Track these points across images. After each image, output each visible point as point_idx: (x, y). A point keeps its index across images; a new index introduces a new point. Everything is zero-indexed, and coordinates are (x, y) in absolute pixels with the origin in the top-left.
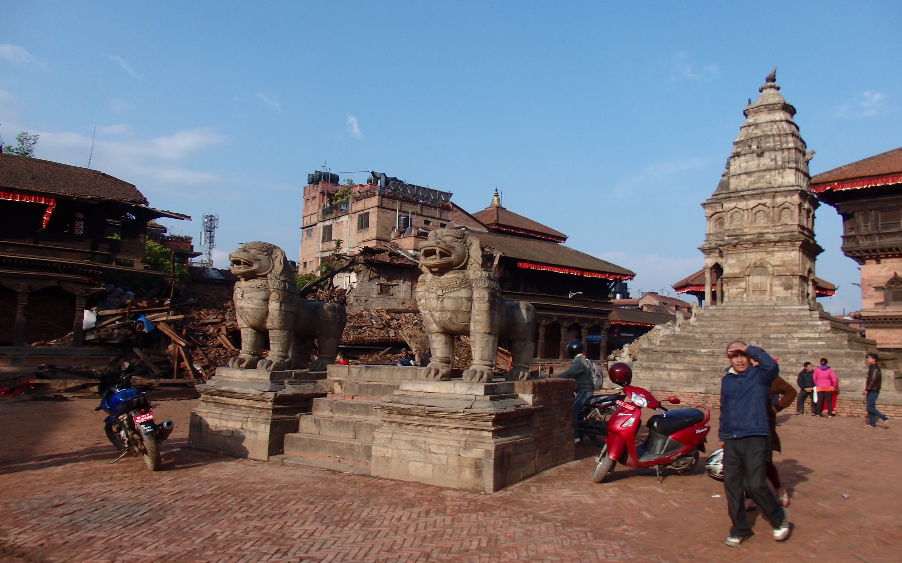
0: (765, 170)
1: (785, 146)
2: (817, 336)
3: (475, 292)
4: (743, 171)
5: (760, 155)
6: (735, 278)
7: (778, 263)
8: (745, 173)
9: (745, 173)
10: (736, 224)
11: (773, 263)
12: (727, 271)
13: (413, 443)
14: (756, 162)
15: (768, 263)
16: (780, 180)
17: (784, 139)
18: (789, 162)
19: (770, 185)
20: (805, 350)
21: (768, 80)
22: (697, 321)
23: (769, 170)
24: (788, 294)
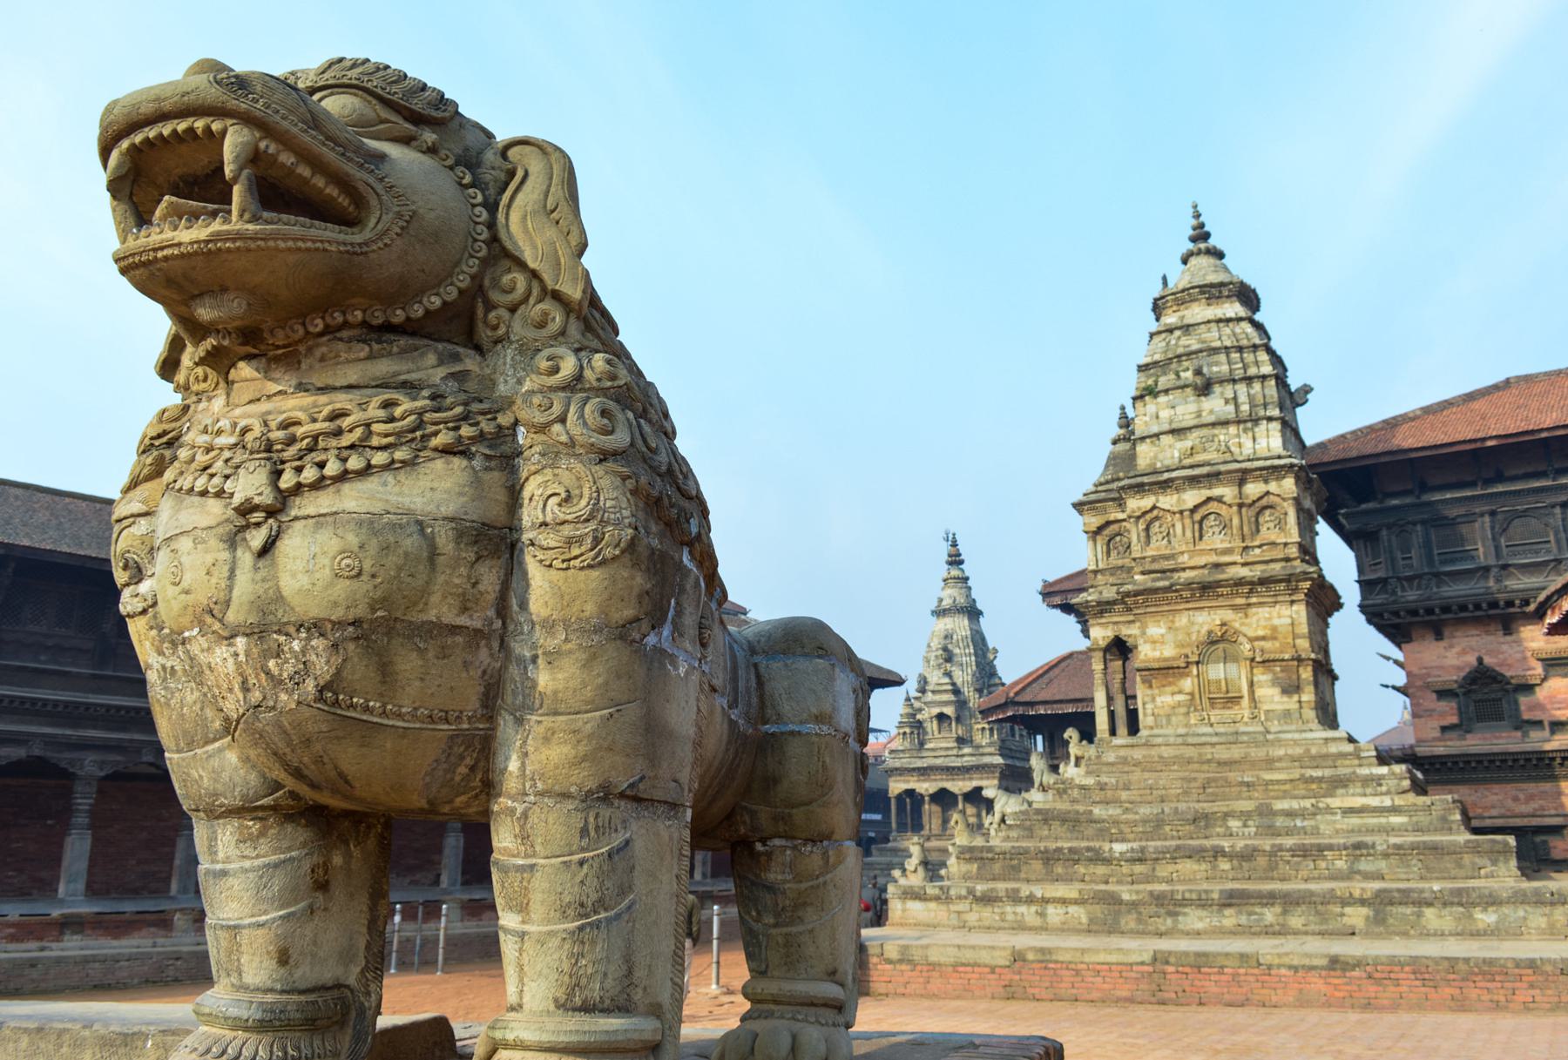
0: (1214, 425)
1: (1252, 371)
2: (1387, 802)
3: (532, 488)
4: (1166, 427)
5: (1205, 389)
6: (1165, 672)
7: (1261, 633)
8: (1172, 432)
9: (1172, 432)
10: (1157, 546)
11: (1251, 634)
12: (1146, 653)
17: (1249, 357)
18: (1265, 406)
19: (1228, 457)
20: (1368, 839)
21: (1193, 239)
22: (1088, 773)
24: (1291, 703)
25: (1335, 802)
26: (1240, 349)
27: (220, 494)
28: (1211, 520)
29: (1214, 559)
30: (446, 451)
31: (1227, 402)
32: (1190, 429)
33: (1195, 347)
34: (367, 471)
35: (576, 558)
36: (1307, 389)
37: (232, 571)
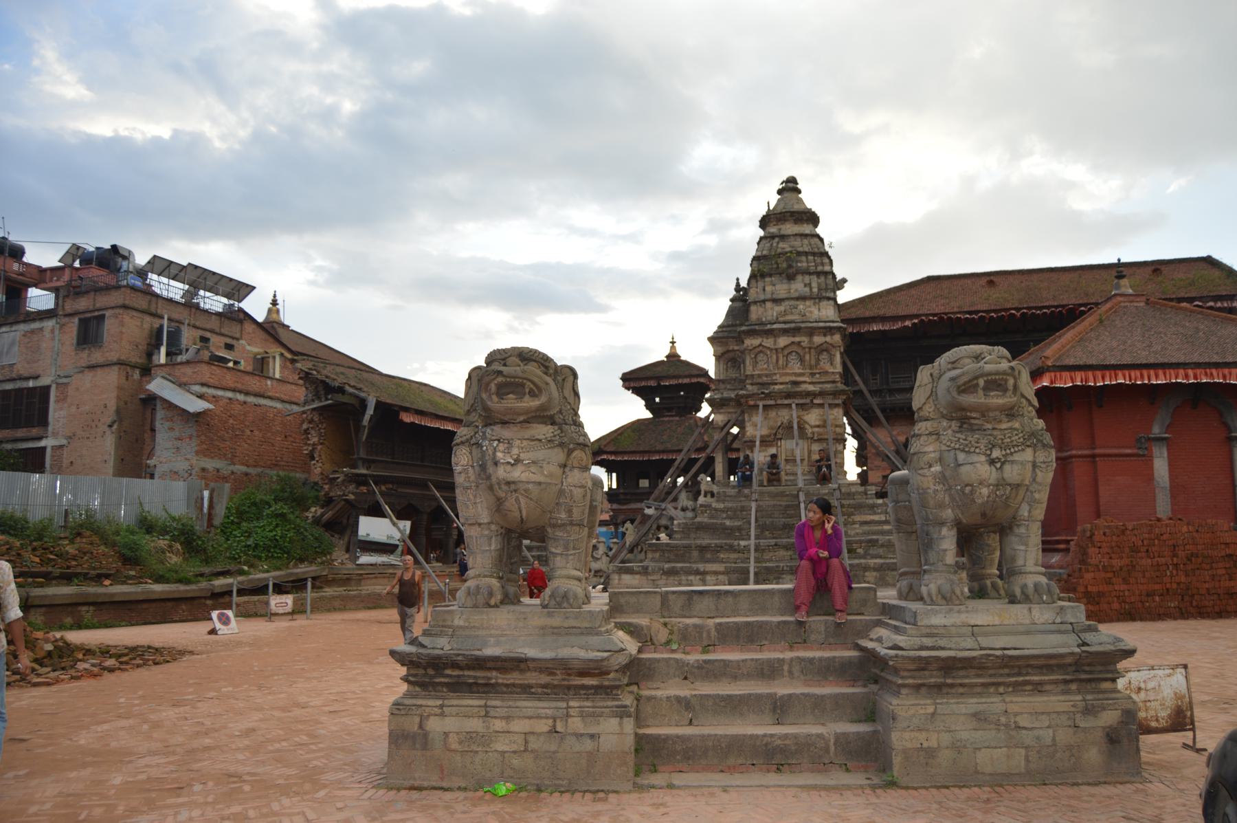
0: (797, 299)
1: (820, 268)
4: (769, 296)
11: (813, 423)
13: (979, 718)
14: (785, 286)
16: (816, 312)
17: (818, 260)
23: (803, 298)
25: (858, 518)
26: (814, 254)
28: (793, 356)
29: (794, 378)
33: (788, 249)
36: (844, 281)
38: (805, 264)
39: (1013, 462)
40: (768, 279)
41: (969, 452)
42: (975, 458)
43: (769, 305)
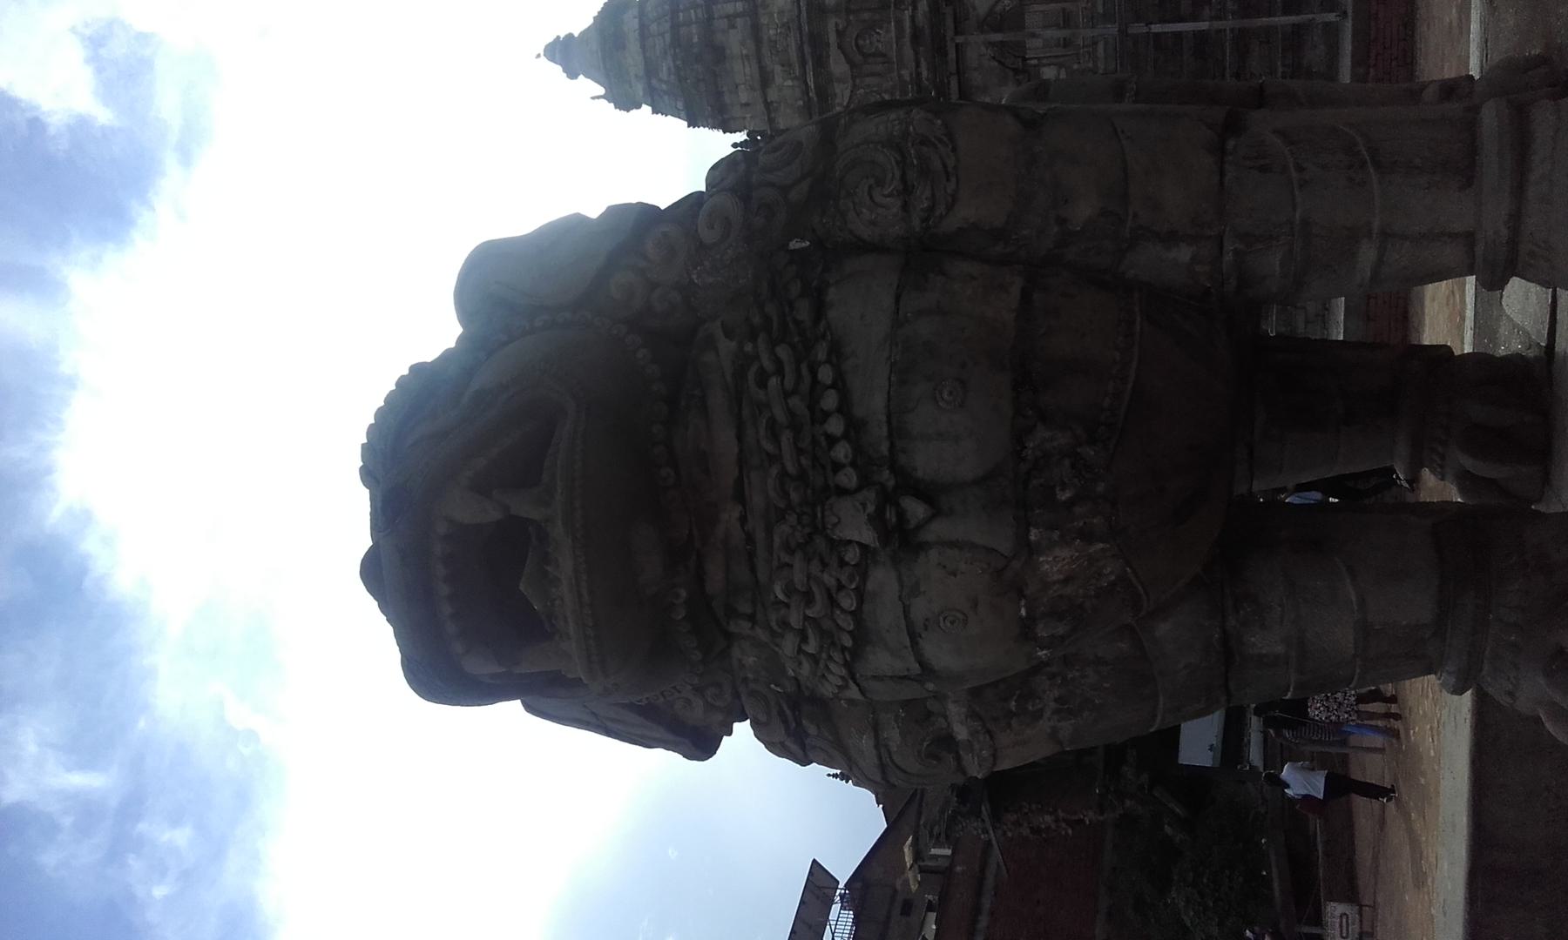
0: (758, 41)
15: (991, 11)
27: (862, 570)
29: (907, 39)
30: (819, 310)
31: (733, 27)
32: (762, 69)
34: (840, 383)
35: (945, 166)
37: (953, 544)
38: (694, 29)
39: (896, 432)
40: (727, 99)
41: (863, 636)
42: (886, 615)
43: (773, 95)
